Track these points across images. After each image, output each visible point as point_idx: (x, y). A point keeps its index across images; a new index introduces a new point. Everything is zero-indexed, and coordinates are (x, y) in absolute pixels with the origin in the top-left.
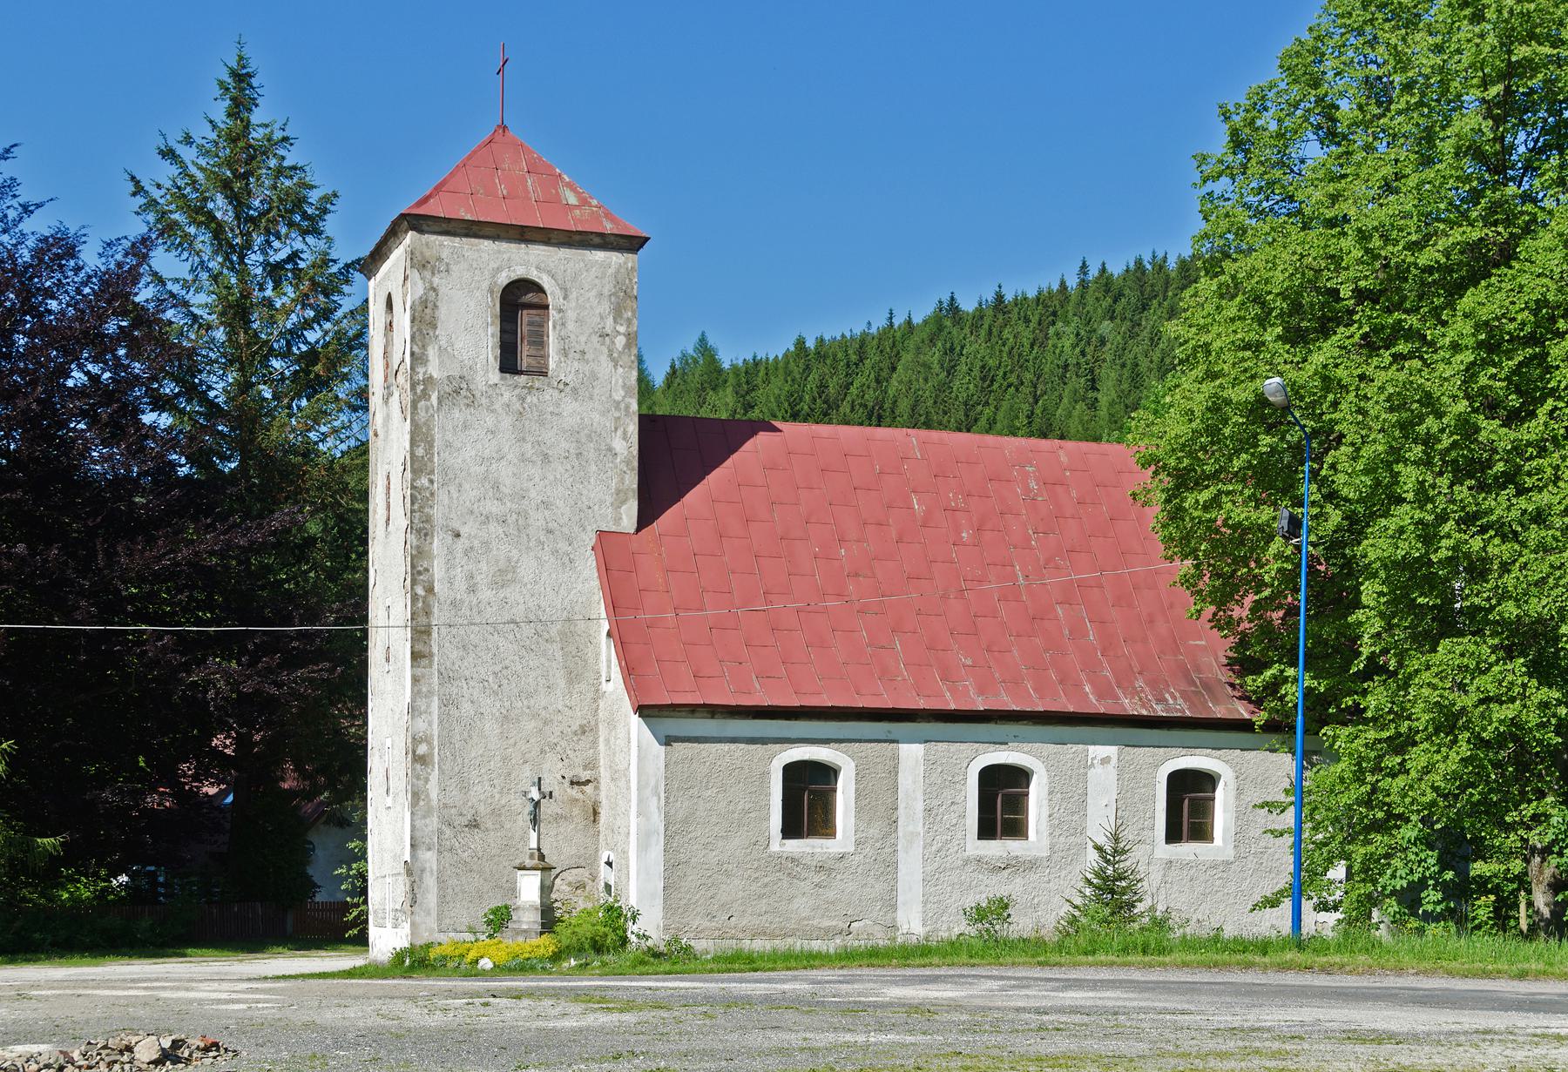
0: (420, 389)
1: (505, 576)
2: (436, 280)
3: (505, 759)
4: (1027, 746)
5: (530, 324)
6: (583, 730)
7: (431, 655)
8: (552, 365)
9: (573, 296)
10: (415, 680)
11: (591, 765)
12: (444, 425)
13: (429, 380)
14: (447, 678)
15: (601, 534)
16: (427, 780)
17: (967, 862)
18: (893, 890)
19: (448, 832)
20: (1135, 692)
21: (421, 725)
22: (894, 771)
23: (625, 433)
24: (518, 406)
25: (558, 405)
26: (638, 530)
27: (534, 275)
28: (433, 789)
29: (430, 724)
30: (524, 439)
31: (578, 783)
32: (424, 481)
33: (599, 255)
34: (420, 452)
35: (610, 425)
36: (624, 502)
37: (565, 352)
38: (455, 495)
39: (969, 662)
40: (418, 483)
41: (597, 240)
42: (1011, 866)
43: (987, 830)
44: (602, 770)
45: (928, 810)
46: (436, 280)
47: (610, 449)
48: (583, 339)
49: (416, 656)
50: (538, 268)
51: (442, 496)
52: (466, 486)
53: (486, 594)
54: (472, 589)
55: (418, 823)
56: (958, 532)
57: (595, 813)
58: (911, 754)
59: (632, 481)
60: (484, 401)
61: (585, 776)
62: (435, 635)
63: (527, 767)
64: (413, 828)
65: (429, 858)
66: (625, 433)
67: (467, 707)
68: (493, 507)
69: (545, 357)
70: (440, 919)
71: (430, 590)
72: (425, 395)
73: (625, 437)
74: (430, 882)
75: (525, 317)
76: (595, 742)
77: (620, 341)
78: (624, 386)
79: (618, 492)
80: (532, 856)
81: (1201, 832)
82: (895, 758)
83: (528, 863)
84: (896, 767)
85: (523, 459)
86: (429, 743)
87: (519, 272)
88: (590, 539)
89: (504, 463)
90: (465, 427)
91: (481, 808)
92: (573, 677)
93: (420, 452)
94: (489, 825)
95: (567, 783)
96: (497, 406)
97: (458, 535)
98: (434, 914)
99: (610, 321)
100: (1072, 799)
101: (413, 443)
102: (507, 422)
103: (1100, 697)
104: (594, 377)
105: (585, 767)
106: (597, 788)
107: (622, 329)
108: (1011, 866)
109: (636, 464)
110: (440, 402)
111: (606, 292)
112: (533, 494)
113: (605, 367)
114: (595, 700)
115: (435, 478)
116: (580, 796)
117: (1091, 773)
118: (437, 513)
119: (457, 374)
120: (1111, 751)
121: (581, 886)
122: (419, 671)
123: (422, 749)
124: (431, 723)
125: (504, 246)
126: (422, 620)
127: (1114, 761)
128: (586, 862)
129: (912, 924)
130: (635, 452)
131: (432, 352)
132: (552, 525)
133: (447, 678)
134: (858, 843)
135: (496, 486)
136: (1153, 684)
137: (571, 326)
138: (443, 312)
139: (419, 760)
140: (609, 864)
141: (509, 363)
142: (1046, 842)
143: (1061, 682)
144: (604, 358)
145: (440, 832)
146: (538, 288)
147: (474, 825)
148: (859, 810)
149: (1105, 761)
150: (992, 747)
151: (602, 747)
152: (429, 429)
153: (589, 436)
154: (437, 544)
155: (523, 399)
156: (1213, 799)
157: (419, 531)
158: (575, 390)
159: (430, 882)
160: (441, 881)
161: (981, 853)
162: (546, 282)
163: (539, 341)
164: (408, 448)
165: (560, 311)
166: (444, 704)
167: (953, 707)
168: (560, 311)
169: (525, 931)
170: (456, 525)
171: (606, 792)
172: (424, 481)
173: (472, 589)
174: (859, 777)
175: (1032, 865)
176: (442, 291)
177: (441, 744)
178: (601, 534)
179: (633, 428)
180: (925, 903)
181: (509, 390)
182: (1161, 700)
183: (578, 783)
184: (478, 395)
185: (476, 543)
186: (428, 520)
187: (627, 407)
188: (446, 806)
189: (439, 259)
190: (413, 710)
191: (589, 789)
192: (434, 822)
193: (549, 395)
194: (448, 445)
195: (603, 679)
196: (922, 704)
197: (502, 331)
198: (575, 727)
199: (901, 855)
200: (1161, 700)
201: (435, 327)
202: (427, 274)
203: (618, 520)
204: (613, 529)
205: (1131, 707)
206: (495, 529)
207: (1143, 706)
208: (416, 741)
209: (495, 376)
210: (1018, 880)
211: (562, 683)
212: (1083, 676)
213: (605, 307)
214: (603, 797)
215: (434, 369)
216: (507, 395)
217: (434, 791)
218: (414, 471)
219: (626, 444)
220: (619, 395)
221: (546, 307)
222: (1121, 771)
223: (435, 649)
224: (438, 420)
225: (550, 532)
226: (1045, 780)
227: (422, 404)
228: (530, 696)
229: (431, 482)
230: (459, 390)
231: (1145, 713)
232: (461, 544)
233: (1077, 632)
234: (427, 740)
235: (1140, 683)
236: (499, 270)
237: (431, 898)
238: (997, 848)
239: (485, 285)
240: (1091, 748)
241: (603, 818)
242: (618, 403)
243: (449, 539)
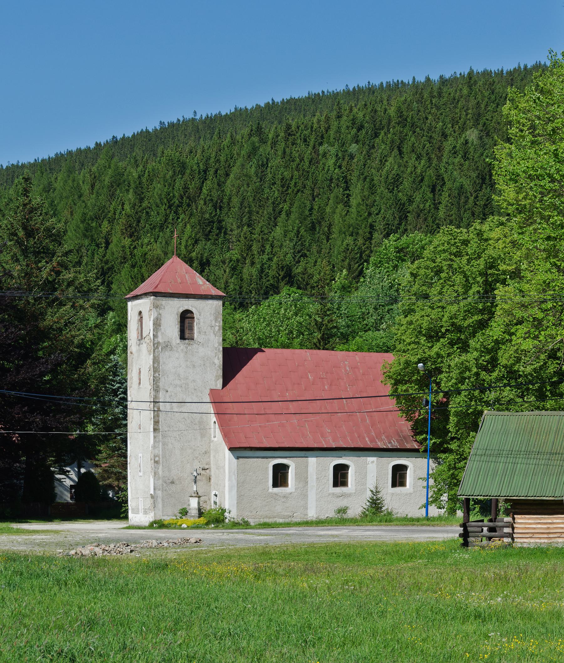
0: (156, 345)
2: (161, 311)
3: (182, 462)
5: (188, 323)
6: (206, 453)
7: (159, 429)
8: (195, 336)
9: (202, 314)
10: (155, 437)
11: (208, 463)
12: (164, 356)
13: (158, 343)
14: (164, 437)
15: (211, 390)
16: (158, 469)
17: (329, 494)
18: (307, 503)
19: (165, 485)
20: (382, 440)
21: (156, 451)
23: (218, 357)
24: (185, 350)
25: (198, 349)
26: (223, 388)
27: (190, 309)
28: (160, 471)
29: (159, 451)
30: (187, 361)
31: (204, 469)
32: (157, 375)
33: (210, 302)
34: (156, 365)
36: (218, 379)
37: (200, 332)
38: (166, 378)
39: (329, 431)
40: (155, 375)
41: (210, 297)
42: (343, 495)
43: (336, 484)
44: (212, 465)
45: (317, 478)
46: (161, 311)
47: (214, 363)
48: (205, 328)
49: (155, 430)
50: (192, 306)
55: (156, 482)
56: (324, 386)
57: (210, 479)
58: (312, 461)
59: (220, 373)
60: (175, 349)
61: (206, 467)
62: (160, 423)
63: (189, 464)
64: (154, 484)
65: (159, 493)
66: (218, 357)
67: (170, 445)
68: (178, 382)
69: (193, 334)
70: (163, 512)
72: (157, 347)
73: (218, 359)
74: (160, 500)
75: (187, 321)
76: (209, 457)
77: (217, 328)
78: (218, 342)
79: (216, 376)
81: (402, 484)
84: (307, 465)
85: (187, 367)
86: (159, 457)
87: (186, 308)
88: (208, 391)
89: (181, 368)
90: (169, 357)
91: (175, 477)
92: (203, 436)
93: (156, 365)
94: (177, 483)
95: (201, 469)
96: (179, 350)
97: (167, 391)
98: (161, 510)
99: (214, 322)
100: (362, 475)
101: (154, 363)
102: (182, 355)
103: (371, 442)
104: (209, 340)
105: (206, 464)
106: (210, 471)
107: (217, 324)
108: (343, 495)
109: (222, 367)
110: (162, 350)
111: (212, 313)
112: (190, 378)
113: (212, 337)
114: (209, 443)
115: (160, 373)
116: (205, 473)
117: (368, 466)
118: (161, 384)
119: (167, 340)
120: (374, 459)
121: (205, 502)
122: (156, 434)
123: (157, 459)
124: (159, 451)
126: (157, 418)
127: (375, 462)
128: (208, 494)
129: (312, 514)
130: (222, 364)
131: (159, 334)
133: (164, 437)
134: (296, 489)
135: (179, 376)
136: (387, 437)
137: (201, 324)
138: (163, 322)
139: (156, 462)
140: (216, 495)
142: (354, 488)
143: (359, 437)
144: (212, 334)
145: (163, 485)
146: (191, 312)
147: (173, 483)
149: (373, 462)
150: (337, 458)
151: (212, 458)
152: (159, 358)
153: (207, 359)
156: (406, 473)
157: (155, 390)
158: (203, 344)
159: (160, 500)
160: (163, 500)
161: (334, 491)
162: (194, 310)
163: (191, 329)
164: (152, 363)
165: (198, 319)
166: (163, 445)
167: (325, 446)
168: (198, 319)
170: (167, 388)
171: (213, 472)
172: (157, 375)
175: (349, 495)
176: (162, 315)
177: (163, 457)
178: (211, 390)
179: (221, 356)
180: (316, 507)
181: (183, 345)
182: (390, 443)
183: (204, 469)
185: (173, 394)
186: (158, 387)
187: (219, 349)
188: (164, 477)
189: (162, 305)
190: (154, 447)
191: (207, 471)
192: (160, 482)
193: (195, 346)
194: (164, 363)
195: (212, 436)
197: (181, 326)
198: (203, 452)
200: (390, 443)
201: (160, 326)
202: (158, 310)
203: (216, 385)
204: (215, 388)
205: (381, 445)
206: (178, 389)
207: (384, 445)
208: (155, 456)
209: (178, 340)
210: (346, 500)
211: (199, 438)
212: (365, 435)
213: (212, 318)
214: (212, 473)
215: (160, 339)
216: (182, 347)
218: (154, 371)
219: (218, 360)
220: (216, 345)
221: (194, 318)
222: (377, 465)
223: (160, 428)
225: (195, 390)
226: (354, 469)
227: (156, 350)
228: (189, 442)
229: (159, 375)
230: (167, 346)
231: (385, 447)
232: (169, 394)
233: (363, 420)
234: (158, 456)
235: (383, 437)
236: (180, 307)
237: (160, 505)
238: (339, 490)
239: (175, 312)
240: (368, 458)
241: (212, 480)
242: (216, 348)
243: (165, 392)
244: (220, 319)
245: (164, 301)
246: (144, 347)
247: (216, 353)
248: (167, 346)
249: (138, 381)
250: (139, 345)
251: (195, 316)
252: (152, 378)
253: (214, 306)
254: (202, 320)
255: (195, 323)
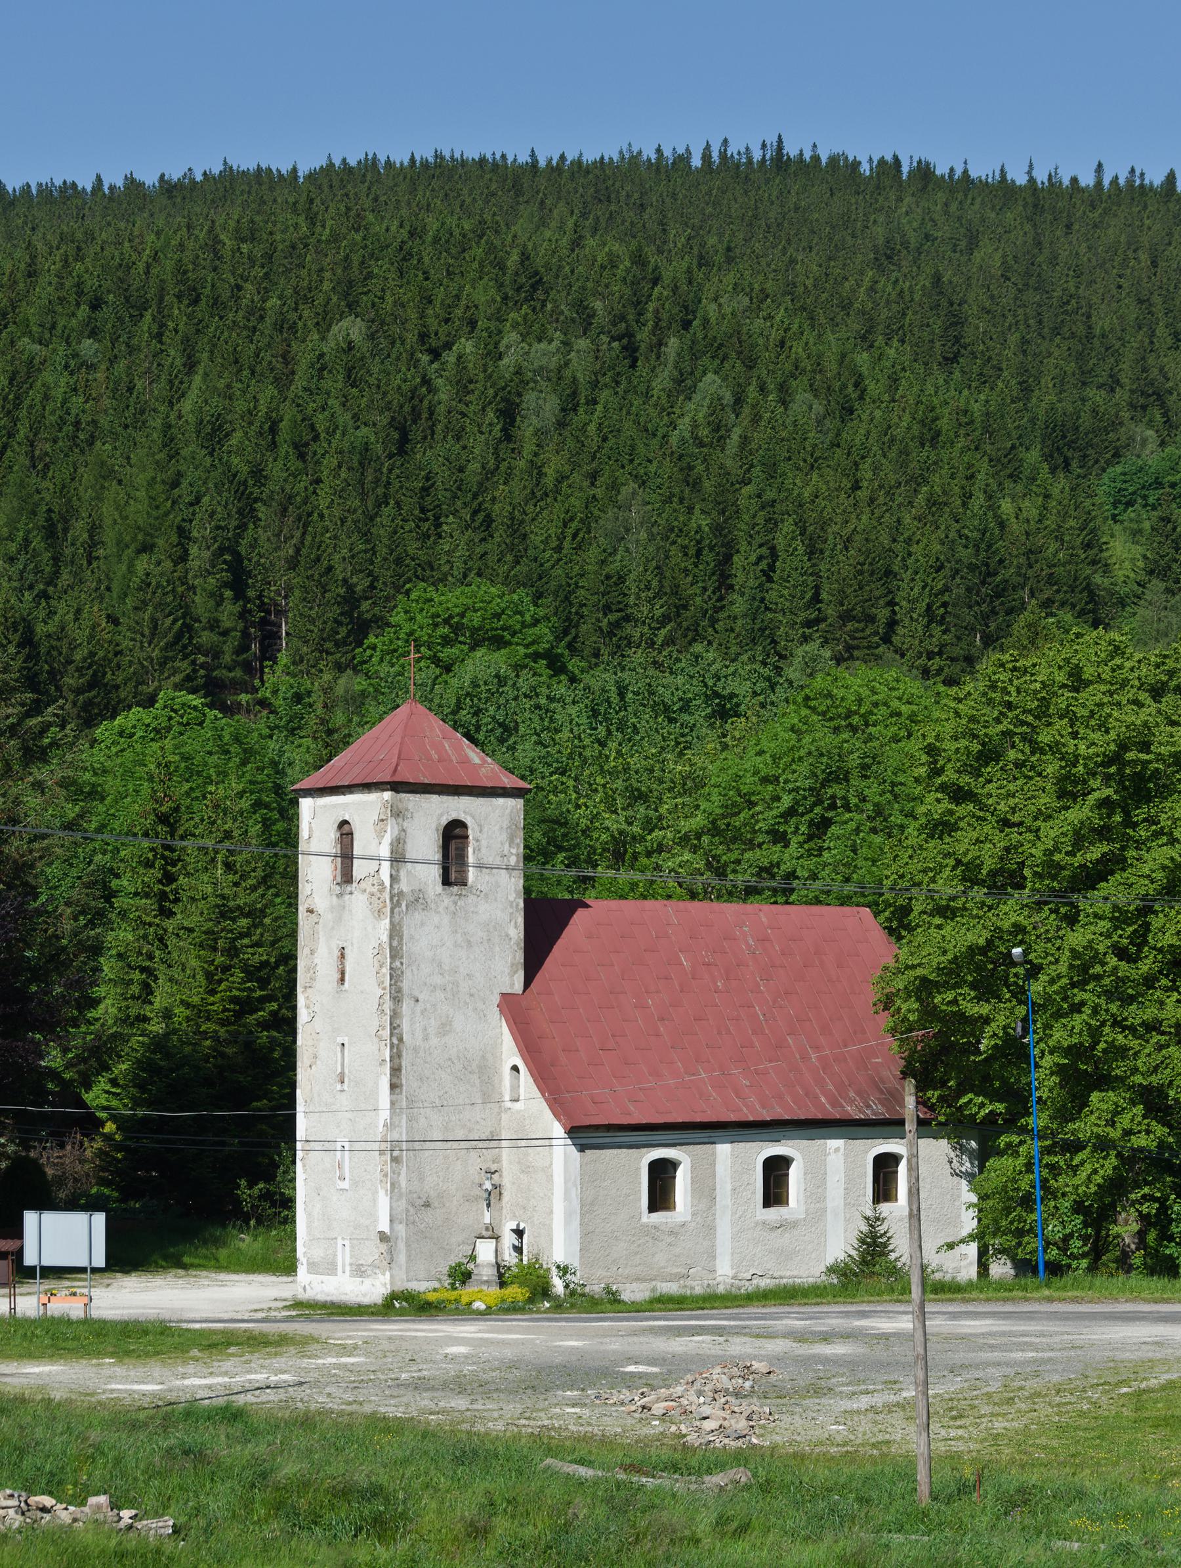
1: (445, 1028)
4: (791, 1143)
9: (485, 830)
12: (412, 922)
13: (401, 893)
17: (757, 1224)
22: (713, 1164)
24: (452, 908)
25: (476, 906)
27: (462, 817)
32: (398, 964)
33: (501, 801)
34: (395, 943)
35: (507, 918)
38: (415, 972)
40: (394, 966)
41: (500, 791)
42: (782, 1226)
46: (405, 824)
49: (393, 1087)
51: (408, 974)
52: (422, 966)
53: (434, 1041)
54: (426, 1039)
58: (724, 1150)
68: (438, 980)
71: (401, 1040)
72: (399, 904)
73: (516, 927)
75: (453, 844)
80: (487, 1229)
82: (714, 1154)
83: (484, 1233)
85: (456, 945)
87: (454, 815)
88: (496, 999)
90: (422, 924)
96: (441, 909)
100: (817, 1179)
101: (391, 937)
102: (446, 919)
107: (514, 851)
115: (404, 961)
118: (405, 985)
119: (417, 888)
125: (445, 798)
132: (473, 991)
135: (440, 965)
137: (484, 851)
141: (446, 882)
142: (803, 1208)
148: (693, 1190)
150: (771, 1144)
152: (401, 927)
154: (406, 1007)
155: (455, 903)
157: (394, 999)
158: (486, 895)
161: (766, 1217)
162: (469, 821)
164: (385, 938)
165: (478, 841)
168: (478, 841)
169: (487, 1282)
170: (416, 993)
173: (426, 1039)
174: (693, 1168)
179: (520, 920)
184: (429, 901)
186: (399, 990)
193: (471, 899)
194: (412, 938)
195: (507, 1097)
196: (732, 1117)
199: (717, 1221)
203: (512, 985)
206: (439, 995)
209: (439, 888)
213: (504, 836)
215: (404, 886)
216: (447, 901)
217: (403, 1183)
218: (391, 957)
219: (516, 931)
220: (512, 897)
221: (467, 837)
224: (406, 921)
226: (802, 1165)
227: (397, 910)
230: (418, 900)
232: (419, 1007)
238: (774, 1213)
244: (519, 841)
245: (411, 800)
246: (358, 901)
247: (511, 914)
248: (418, 900)
249: (338, 976)
250: (340, 895)
251: (470, 832)
252: (386, 971)
253: (508, 811)
254: (484, 843)
255: (470, 850)
